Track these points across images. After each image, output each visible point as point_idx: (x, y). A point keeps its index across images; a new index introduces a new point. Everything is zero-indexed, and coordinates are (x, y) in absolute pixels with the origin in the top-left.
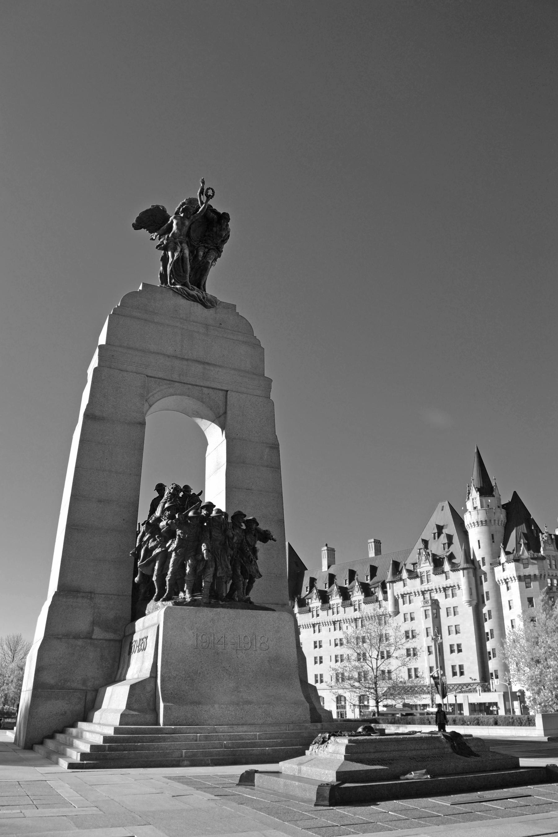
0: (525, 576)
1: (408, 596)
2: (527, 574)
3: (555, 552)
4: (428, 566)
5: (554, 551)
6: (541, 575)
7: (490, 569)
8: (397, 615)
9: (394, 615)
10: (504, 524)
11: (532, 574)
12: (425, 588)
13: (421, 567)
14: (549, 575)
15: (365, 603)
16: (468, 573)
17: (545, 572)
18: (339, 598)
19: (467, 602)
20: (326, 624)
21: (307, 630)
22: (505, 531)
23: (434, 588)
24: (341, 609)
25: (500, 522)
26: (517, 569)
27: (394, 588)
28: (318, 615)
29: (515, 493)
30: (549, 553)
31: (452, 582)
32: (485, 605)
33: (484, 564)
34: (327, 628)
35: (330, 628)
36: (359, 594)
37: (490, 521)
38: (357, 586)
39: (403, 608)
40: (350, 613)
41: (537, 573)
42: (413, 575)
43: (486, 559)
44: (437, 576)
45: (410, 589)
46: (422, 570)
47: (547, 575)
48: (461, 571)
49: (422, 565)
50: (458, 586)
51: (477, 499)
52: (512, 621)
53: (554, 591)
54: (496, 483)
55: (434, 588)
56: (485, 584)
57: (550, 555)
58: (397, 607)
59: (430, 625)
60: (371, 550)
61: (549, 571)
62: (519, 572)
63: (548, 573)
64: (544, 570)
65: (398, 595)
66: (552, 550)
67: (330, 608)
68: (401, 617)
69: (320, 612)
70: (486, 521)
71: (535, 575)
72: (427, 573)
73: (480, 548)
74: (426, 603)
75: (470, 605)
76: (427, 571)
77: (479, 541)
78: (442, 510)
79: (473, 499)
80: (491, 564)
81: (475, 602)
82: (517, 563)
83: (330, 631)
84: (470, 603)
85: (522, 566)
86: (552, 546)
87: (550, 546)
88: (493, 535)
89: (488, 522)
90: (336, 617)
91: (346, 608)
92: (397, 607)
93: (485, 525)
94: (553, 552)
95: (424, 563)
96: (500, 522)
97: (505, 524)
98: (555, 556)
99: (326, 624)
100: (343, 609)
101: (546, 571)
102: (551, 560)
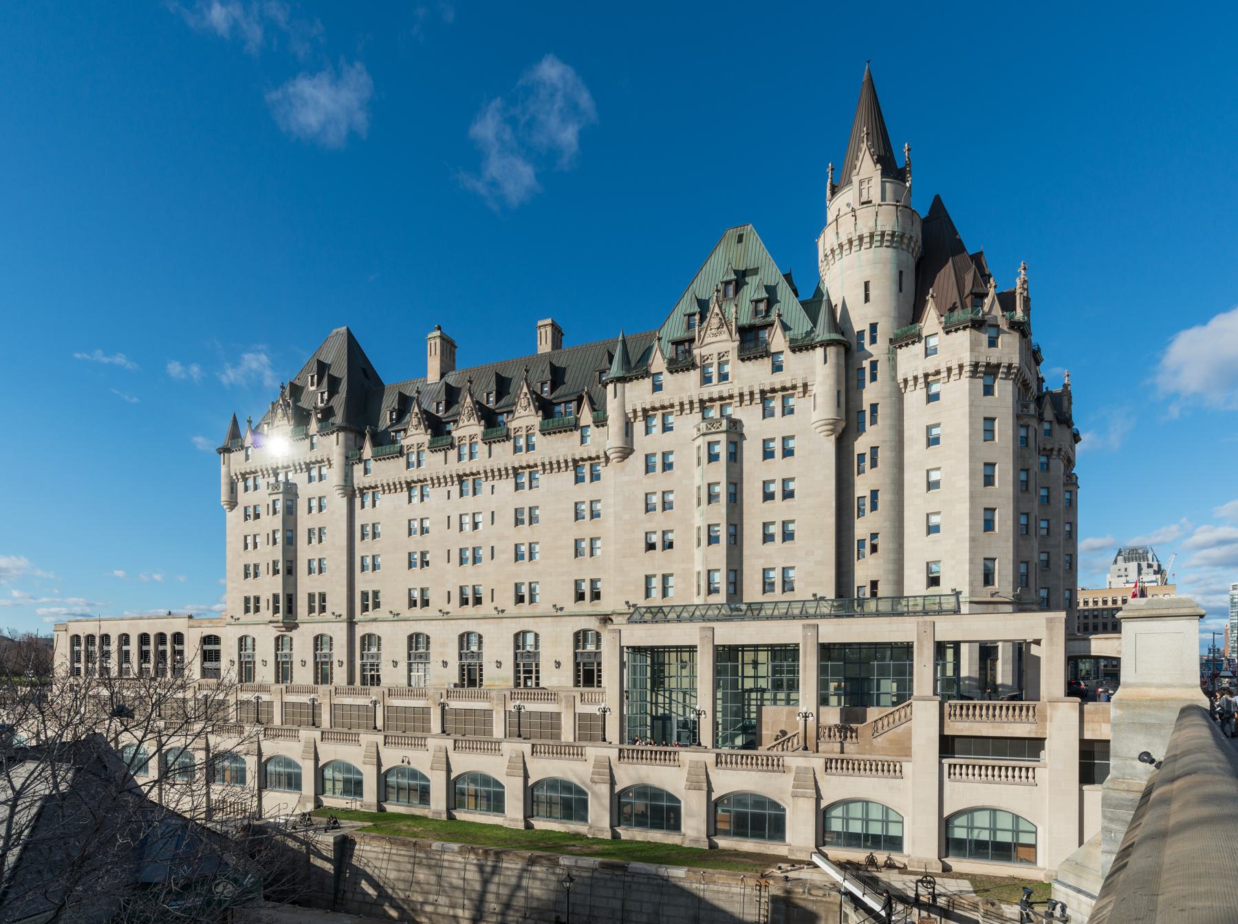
0: (988, 364)
1: (659, 413)
2: (994, 361)
4: (726, 341)
13: (704, 344)
15: (544, 432)
18: (477, 422)
20: (437, 481)
21: (393, 495)
23: (736, 393)
24: (481, 448)
26: (974, 346)
27: (627, 394)
31: (789, 378)
33: (873, 340)
34: (443, 491)
35: (449, 492)
36: (530, 413)
38: (526, 394)
40: (503, 454)
42: (682, 362)
44: (747, 363)
45: (669, 397)
46: (705, 351)
48: (819, 351)
49: (707, 340)
51: (872, 183)
55: (736, 393)
60: (543, 342)
62: (976, 354)
65: (635, 411)
67: (452, 446)
68: (636, 461)
71: (1010, 367)
72: (720, 359)
76: (719, 354)
79: (861, 182)
80: (891, 341)
82: (975, 332)
83: (449, 498)
88: (901, 273)
90: (466, 466)
91: (494, 446)
95: (715, 335)
99: (437, 481)
100: (486, 447)
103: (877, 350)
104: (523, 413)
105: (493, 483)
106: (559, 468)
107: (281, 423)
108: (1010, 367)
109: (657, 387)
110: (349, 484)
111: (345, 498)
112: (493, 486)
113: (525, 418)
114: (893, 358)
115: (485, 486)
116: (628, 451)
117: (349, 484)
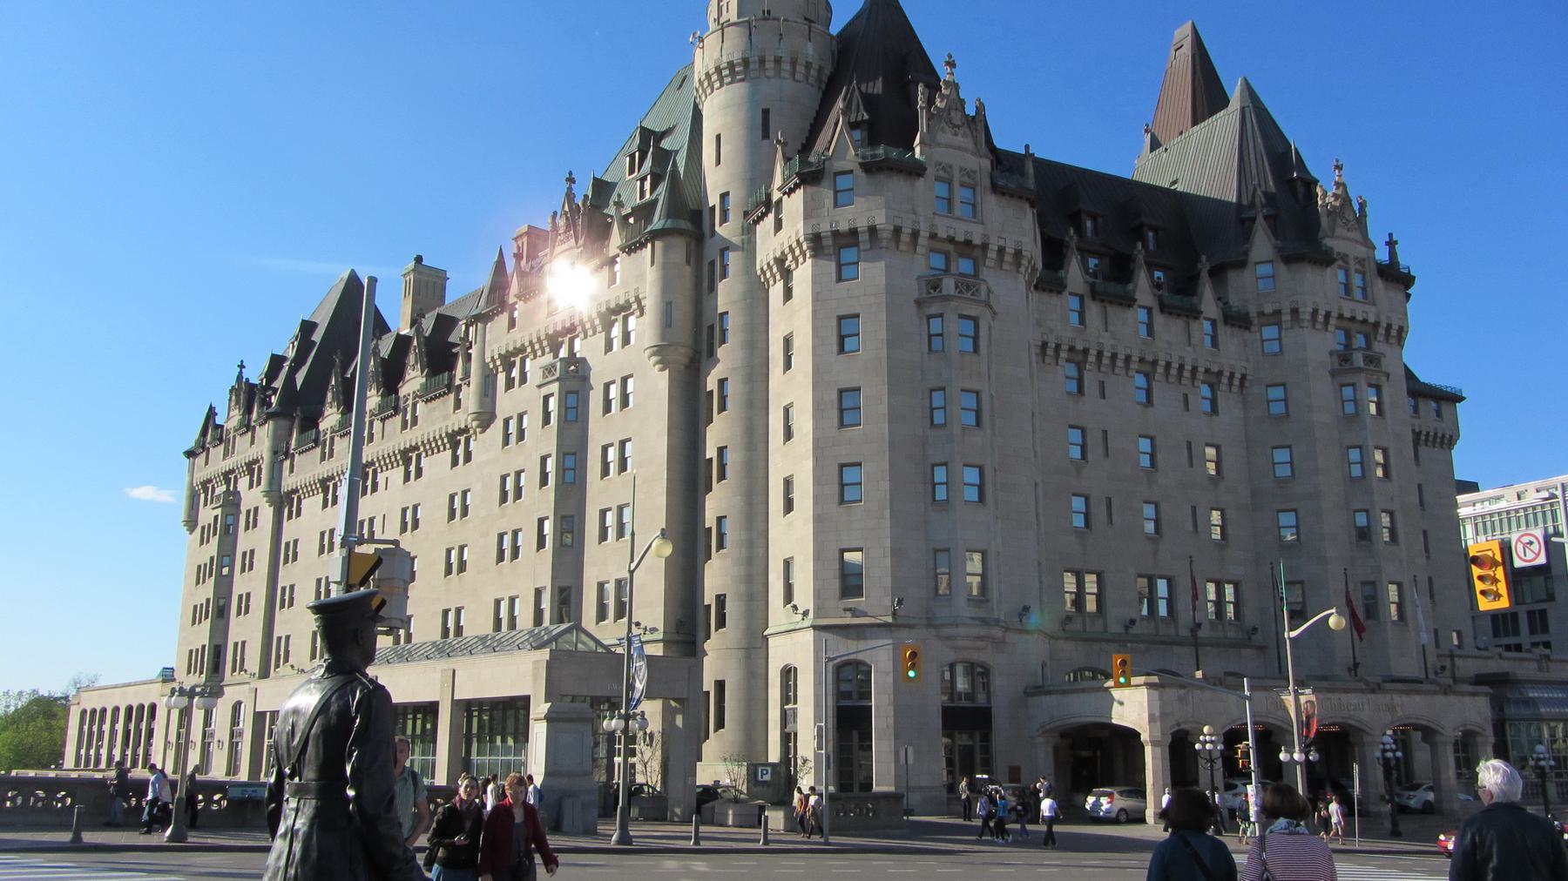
0: (836, 234)
2: (844, 227)
3: (973, 158)
5: (973, 153)
6: (897, 231)
7: (740, 231)
8: (488, 426)
9: (478, 426)
10: (819, 80)
11: (862, 224)
12: (555, 324)
14: (933, 236)
16: (666, 250)
17: (914, 222)
19: (654, 354)
22: (820, 106)
25: (800, 69)
30: (940, 154)
32: (718, 361)
33: (724, 219)
37: (762, 61)
39: (506, 403)
41: (880, 219)
43: (731, 198)
47: (924, 234)
48: (649, 245)
50: (638, 300)
53: (945, 292)
56: (722, 287)
57: (951, 167)
58: (488, 400)
61: (937, 220)
62: (814, 221)
63: (933, 225)
64: (915, 213)
66: (965, 150)
70: (746, 62)
71: (873, 230)
74: (550, 372)
75: (664, 364)
81: (681, 356)
82: (809, 189)
84: (662, 352)
85: (826, 194)
86: (964, 135)
87: (956, 134)
89: (752, 66)
92: (488, 400)
93: (743, 80)
94: (968, 156)
96: (800, 69)
97: (825, 79)
98: (975, 172)
101: (921, 219)
102: (956, 185)
103: (726, 231)
105: (386, 474)
108: (873, 230)
109: (512, 323)
110: (275, 487)
111: (272, 508)
113: (414, 380)
114: (749, 239)
116: (486, 417)
117: (275, 487)
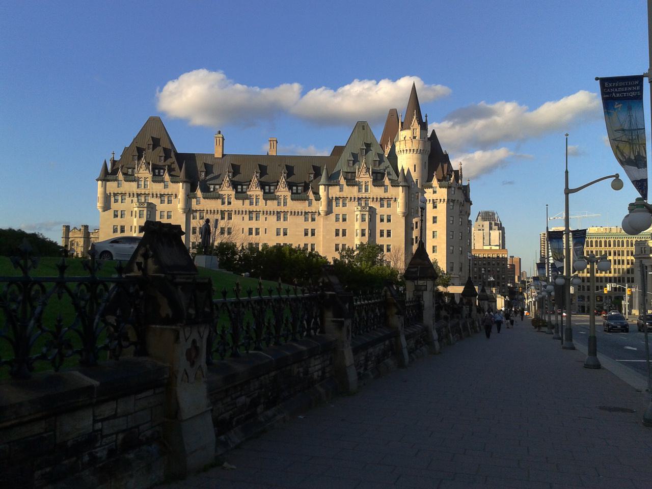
18: (260, 190)
23: (372, 197)
24: (262, 202)
27: (330, 191)
28: (229, 203)
29: (434, 130)
34: (240, 217)
38: (284, 182)
40: (272, 205)
42: (351, 182)
52: (434, 232)
54: (426, 120)
59: (366, 226)
67: (247, 198)
68: (332, 217)
69: (233, 200)
70: (423, 150)
73: (415, 171)
77: (415, 165)
78: (364, 129)
91: (268, 201)
100: (264, 201)
104: (282, 190)
105: (266, 216)
106: (298, 214)
107: (144, 172)
112: (266, 218)
115: (262, 217)
